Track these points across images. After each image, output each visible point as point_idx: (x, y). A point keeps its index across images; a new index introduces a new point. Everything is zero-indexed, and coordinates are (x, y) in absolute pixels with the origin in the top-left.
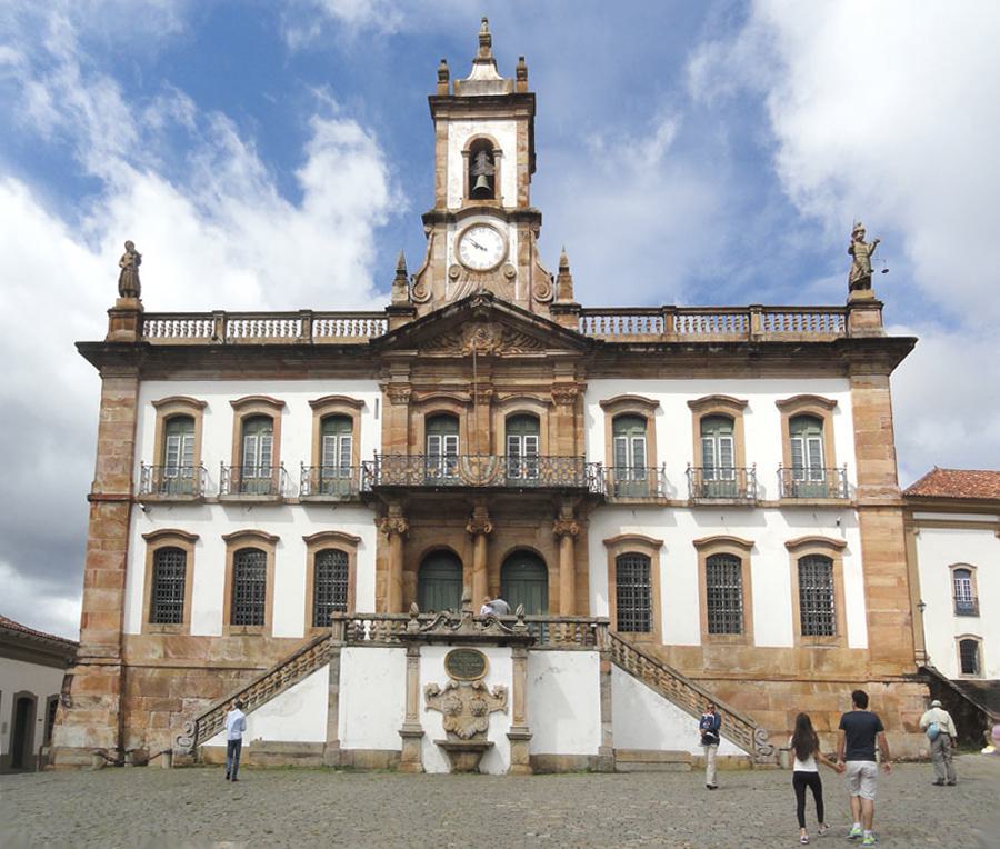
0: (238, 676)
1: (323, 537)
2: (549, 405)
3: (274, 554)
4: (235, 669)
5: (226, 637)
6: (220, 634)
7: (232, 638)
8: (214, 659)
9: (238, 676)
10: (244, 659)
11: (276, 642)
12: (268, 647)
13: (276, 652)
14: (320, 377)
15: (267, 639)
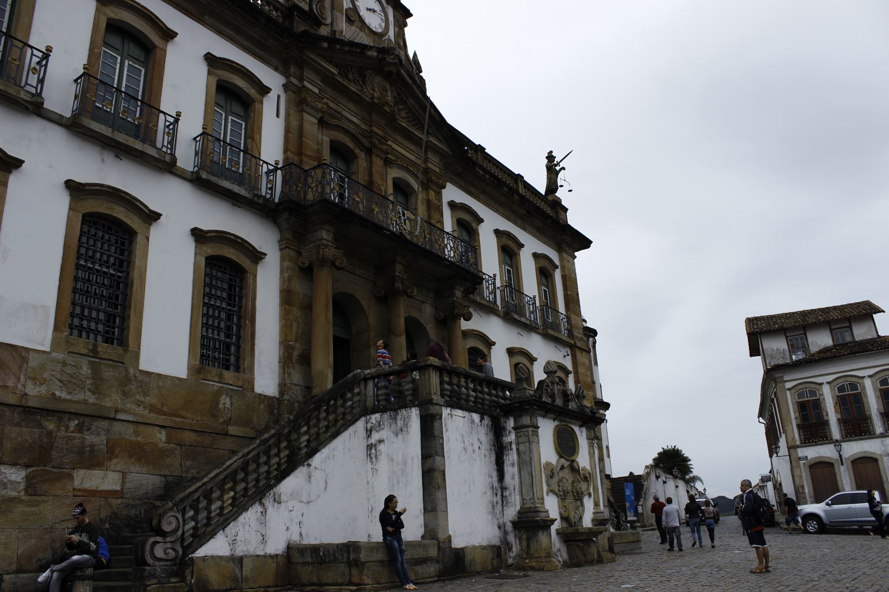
0: (80, 428)
1: (222, 237)
2: (426, 186)
3: (148, 239)
4: (77, 415)
5: (60, 356)
6: (46, 348)
7: (70, 359)
8: (32, 390)
9: (80, 428)
10: (92, 399)
11: (146, 379)
12: (133, 386)
13: (145, 394)
14: (219, 33)
15: (131, 371)
